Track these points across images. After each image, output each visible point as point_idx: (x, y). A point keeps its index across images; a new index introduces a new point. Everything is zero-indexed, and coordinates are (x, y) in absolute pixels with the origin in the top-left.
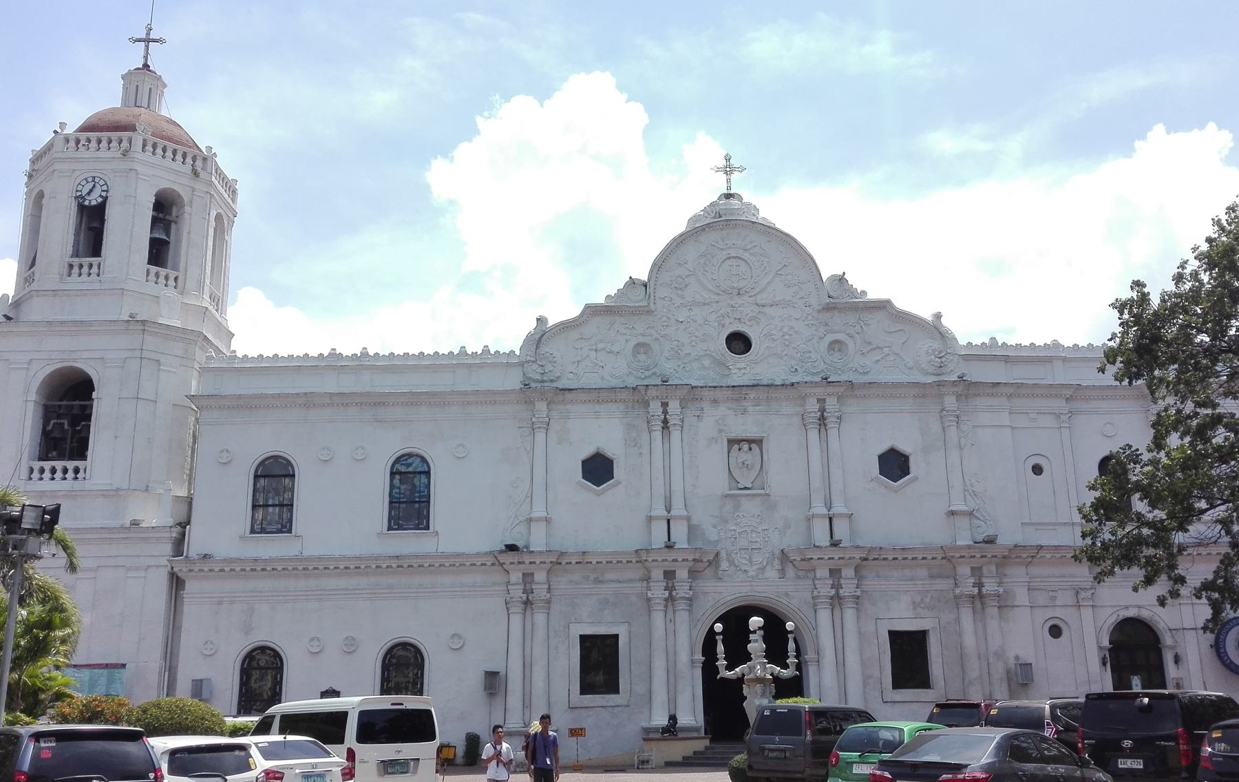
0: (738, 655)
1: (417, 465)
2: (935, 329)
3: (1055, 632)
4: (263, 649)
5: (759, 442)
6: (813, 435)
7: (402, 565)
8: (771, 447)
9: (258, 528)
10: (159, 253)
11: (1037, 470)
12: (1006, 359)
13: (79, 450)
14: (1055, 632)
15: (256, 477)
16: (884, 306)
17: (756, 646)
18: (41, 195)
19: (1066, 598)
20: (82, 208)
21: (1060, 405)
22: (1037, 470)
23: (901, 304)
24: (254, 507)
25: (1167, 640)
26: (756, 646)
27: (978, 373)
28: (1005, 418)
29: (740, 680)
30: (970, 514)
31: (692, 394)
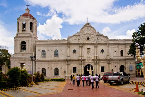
0: (89, 69)
1: (57, 51)
2: (106, 37)
3: (115, 66)
4: (44, 68)
5: (90, 49)
6: (95, 48)
7: (56, 61)
8: (91, 49)
9: (42, 57)
10: (31, 29)
11: (115, 51)
12: (113, 41)
13: (25, 49)
14: (115, 66)
15: (42, 52)
16: (102, 35)
17: (90, 68)
18: (19, 23)
19: (117, 63)
20: (23, 24)
21: (117, 45)
22: (115, 51)
23: (104, 35)
24: (42, 55)
25: (125, 67)
26: (90, 68)
27: (110, 42)
28: (113, 46)
29: (89, 71)
30: (109, 56)
31: (83, 44)
